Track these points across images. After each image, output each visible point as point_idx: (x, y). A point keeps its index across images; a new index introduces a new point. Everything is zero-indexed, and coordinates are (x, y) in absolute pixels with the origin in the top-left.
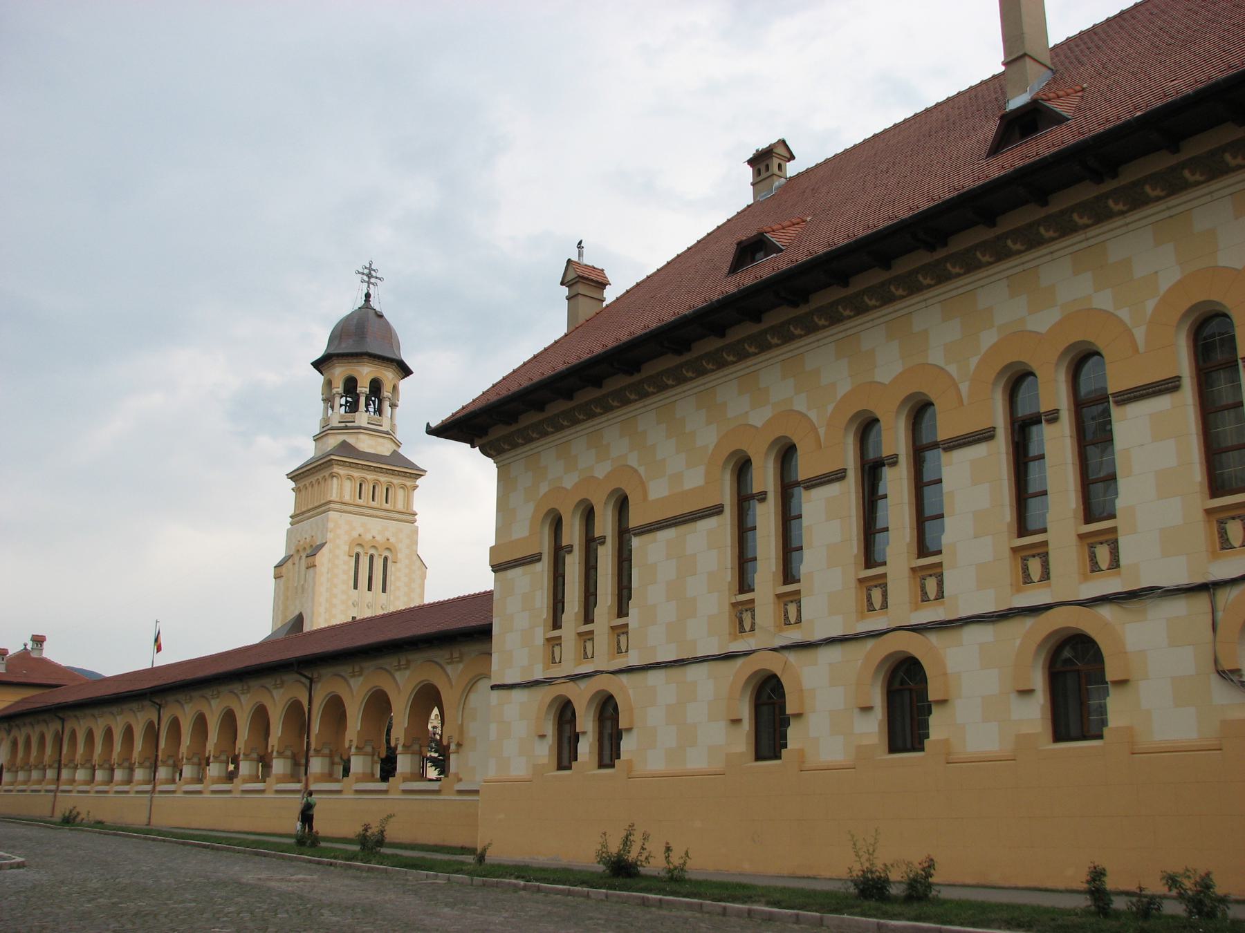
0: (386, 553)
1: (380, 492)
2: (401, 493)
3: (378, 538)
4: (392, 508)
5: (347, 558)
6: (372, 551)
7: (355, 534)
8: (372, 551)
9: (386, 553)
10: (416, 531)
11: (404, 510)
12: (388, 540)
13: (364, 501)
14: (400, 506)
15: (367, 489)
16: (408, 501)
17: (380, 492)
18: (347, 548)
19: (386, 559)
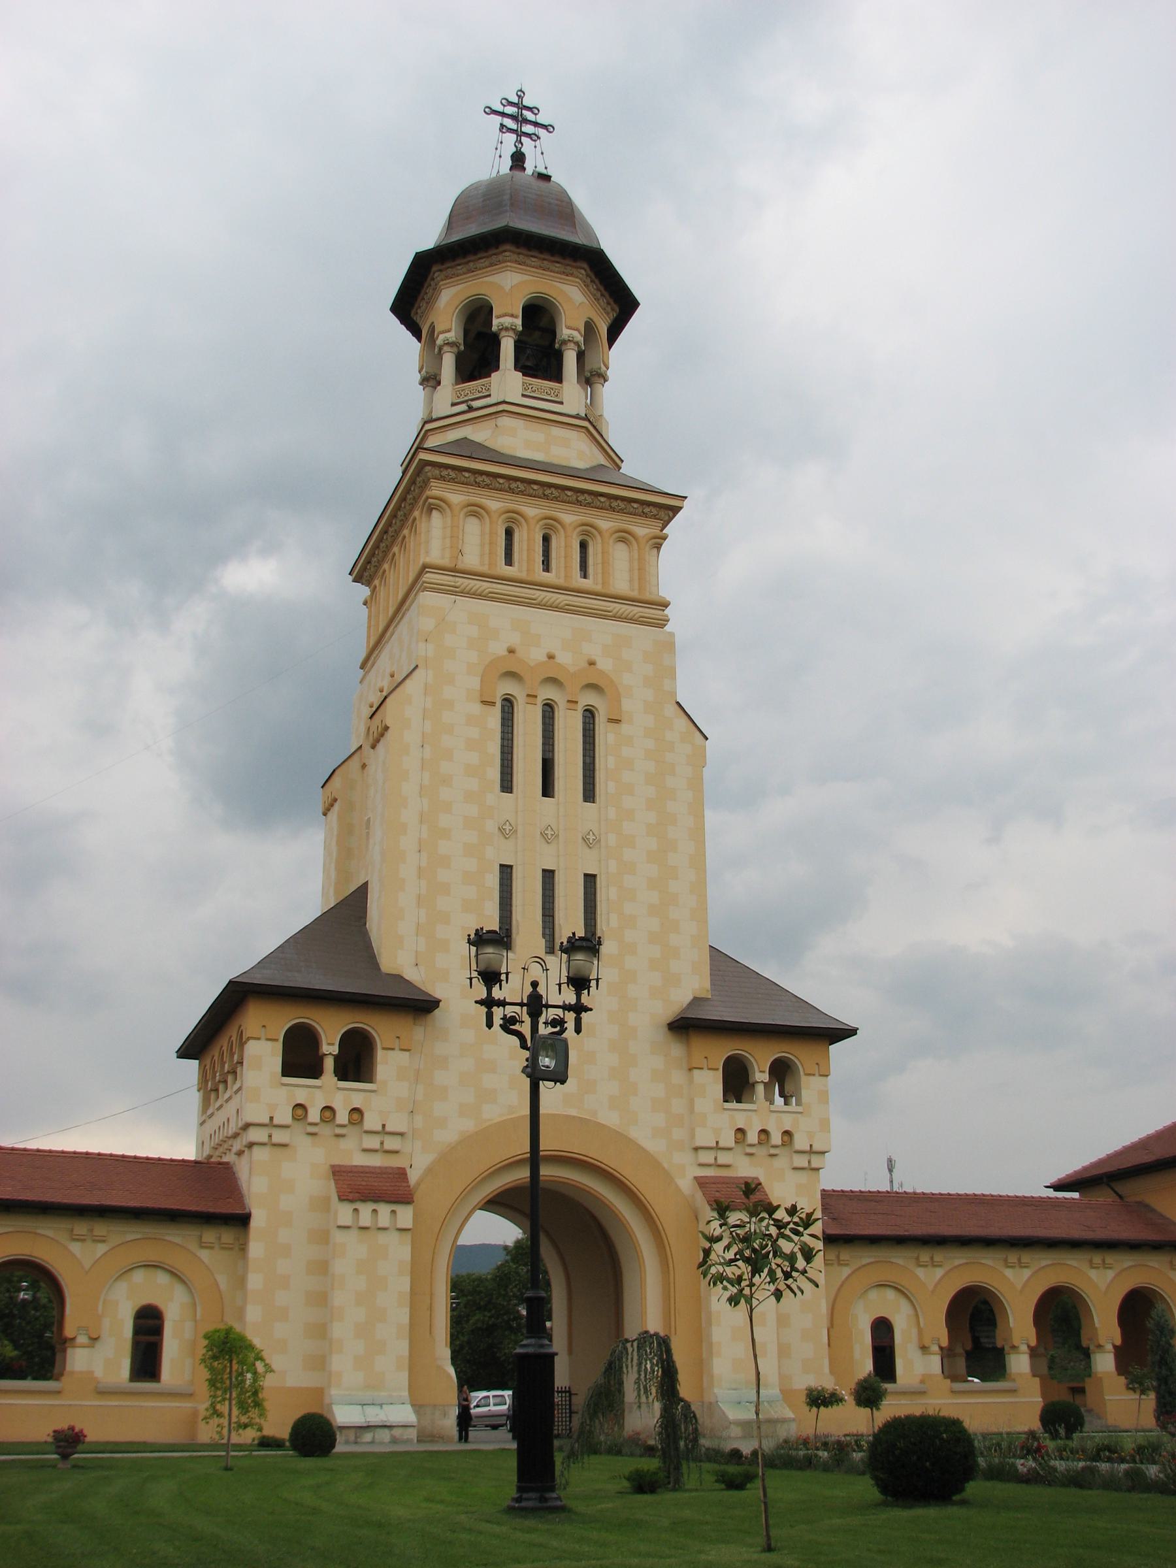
0: (589, 699)
1: (565, 549)
2: (620, 556)
3: (565, 658)
4: (598, 588)
5: (476, 708)
6: (548, 693)
7: (498, 648)
8: (548, 693)
9: (589, 699)
10: (669, 645)
11: (635, 594)
12: (592, 663)
13: (520, 571)
14: (621, 583)
15: (527, 543)
16: (643, 572)
17: (565, 549)
18: (475, 683)
19: (589, 715)
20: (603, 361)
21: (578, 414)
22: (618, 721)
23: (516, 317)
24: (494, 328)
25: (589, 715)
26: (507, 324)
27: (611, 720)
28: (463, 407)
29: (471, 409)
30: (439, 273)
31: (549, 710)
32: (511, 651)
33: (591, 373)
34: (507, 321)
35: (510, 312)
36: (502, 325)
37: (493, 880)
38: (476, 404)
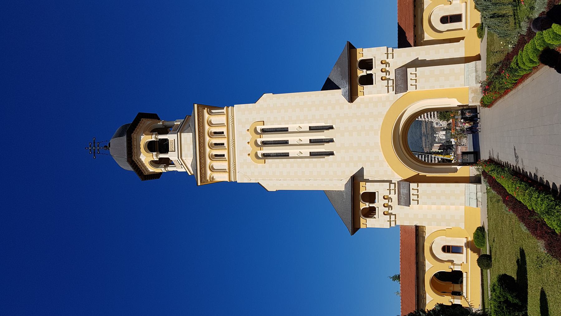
27: (264, 125)
28: (182, 166)
29: (182, 164)
32: (249, 154)
38: (180, 163)
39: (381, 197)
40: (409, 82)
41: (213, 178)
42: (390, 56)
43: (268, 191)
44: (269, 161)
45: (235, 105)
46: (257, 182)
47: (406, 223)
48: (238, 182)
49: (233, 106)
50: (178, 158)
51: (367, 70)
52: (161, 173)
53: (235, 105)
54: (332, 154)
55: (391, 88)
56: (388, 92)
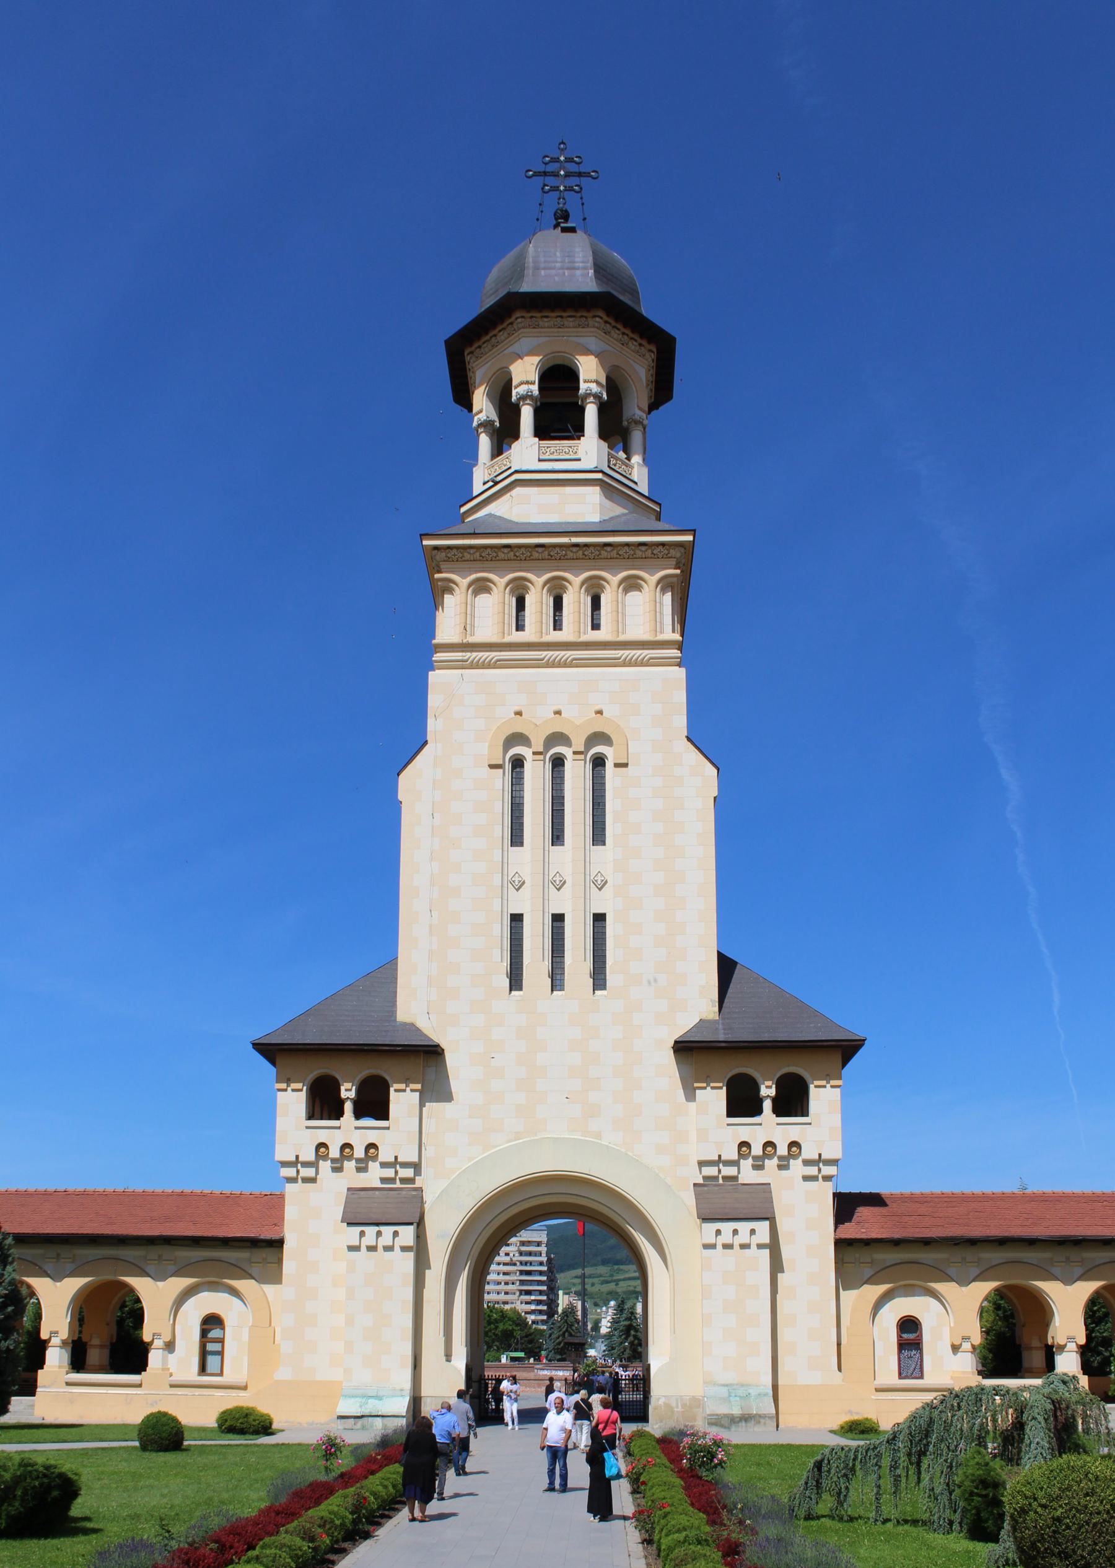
20: (638, 406)
21: (596, 467)
22: (626, 765)
23: (533, 383)
24: (514, 399)
25: (599, 762)
26: (522, 392)
27: (617, 765)
28: (491, 484)
29: (496, 483)
30: (471, 355)
31: (558, 762)
33: (627, 421)
34: (523, 390)
35: (525, 380)
36: (532, 392)
37: (501, 931)
39: (372, 1137)
40: (727, 1227)
41: (450, 591)
42: (812, 1171)
43: (398, 775)
44: (501, 781)
45: (683, 671)
46: (428, 738)
47: (291, 1212)
48: (430, 673)
49: (679, 665)
50: (516, 472)
51: (775, 1101)
52: (469, 407)
53: (683, 671)
54: (516, 981)
55: (711, 1171)
56: (702, 1164)
